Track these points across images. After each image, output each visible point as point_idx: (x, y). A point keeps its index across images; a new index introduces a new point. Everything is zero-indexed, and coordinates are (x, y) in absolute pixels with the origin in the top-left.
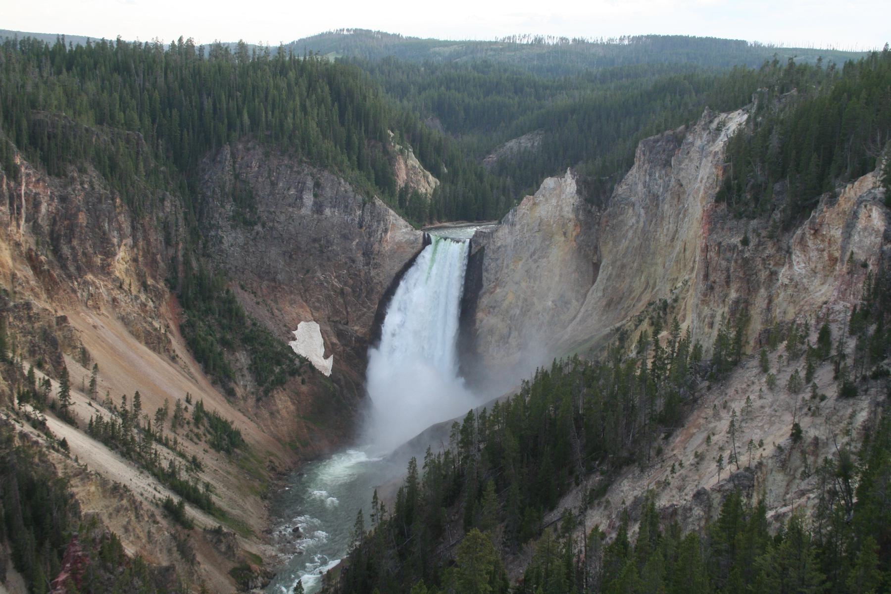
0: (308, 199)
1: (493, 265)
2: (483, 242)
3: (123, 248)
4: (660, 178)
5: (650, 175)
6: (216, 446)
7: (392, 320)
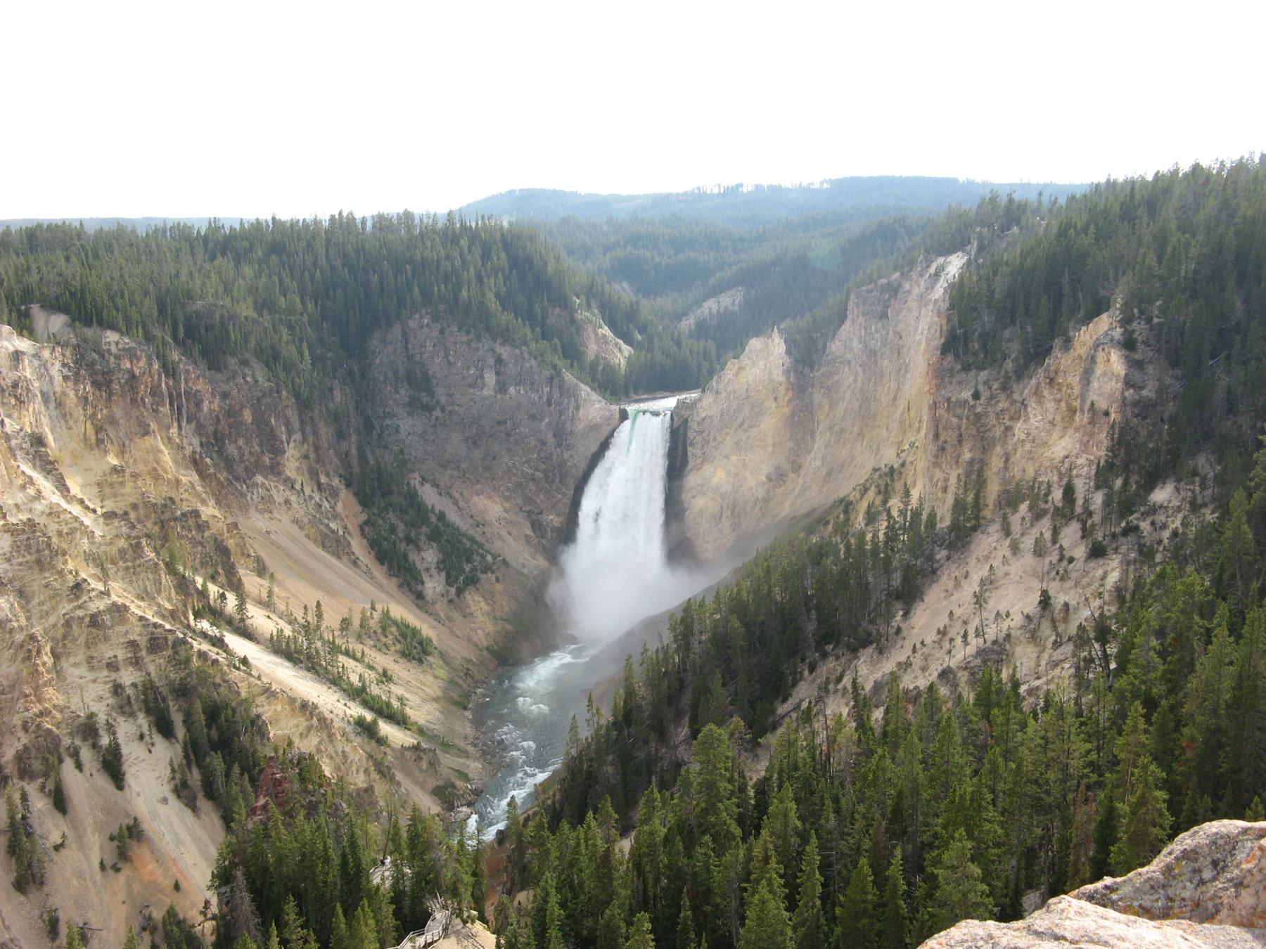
0: (490, 378)
1: (699, 438)
2: (686, 413)
6: (406, 655)
7: (588, 505)
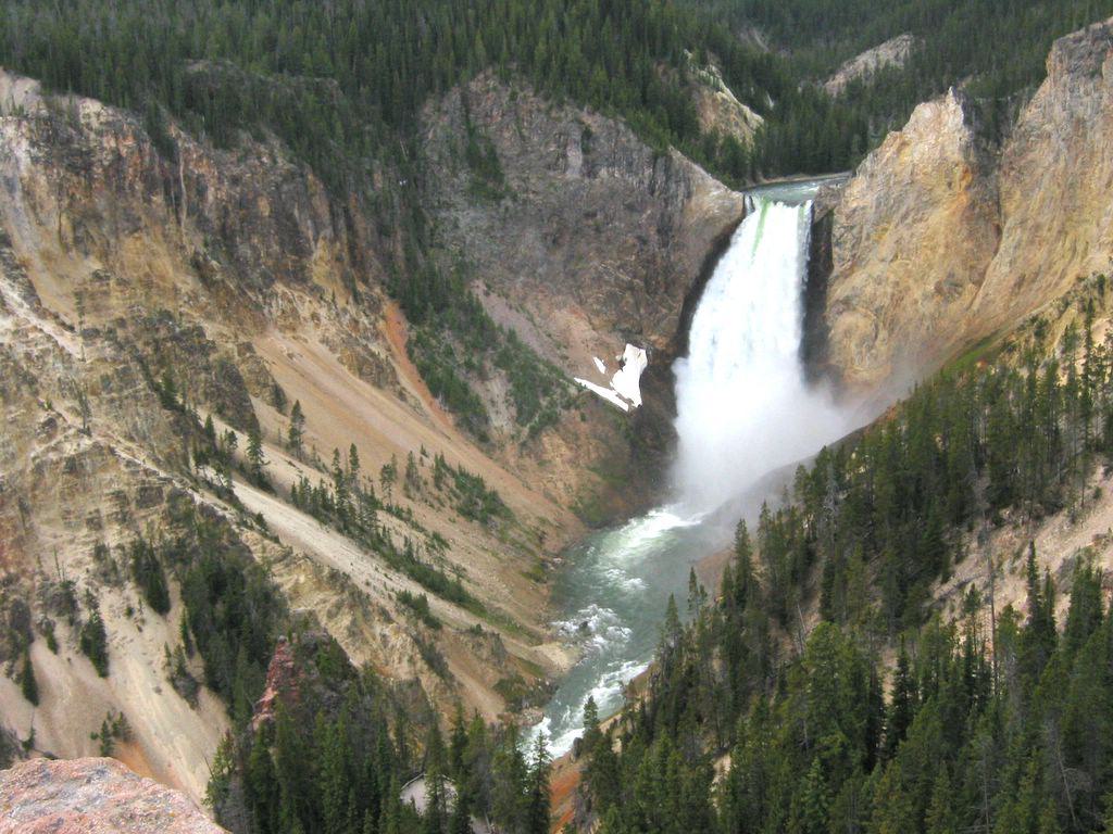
0: (575, 157)
3: (321, 243)
4: (1087, 94)
5: (1072, 92)
6: (467, 513)
